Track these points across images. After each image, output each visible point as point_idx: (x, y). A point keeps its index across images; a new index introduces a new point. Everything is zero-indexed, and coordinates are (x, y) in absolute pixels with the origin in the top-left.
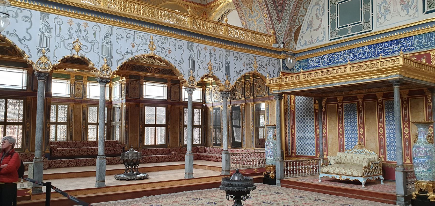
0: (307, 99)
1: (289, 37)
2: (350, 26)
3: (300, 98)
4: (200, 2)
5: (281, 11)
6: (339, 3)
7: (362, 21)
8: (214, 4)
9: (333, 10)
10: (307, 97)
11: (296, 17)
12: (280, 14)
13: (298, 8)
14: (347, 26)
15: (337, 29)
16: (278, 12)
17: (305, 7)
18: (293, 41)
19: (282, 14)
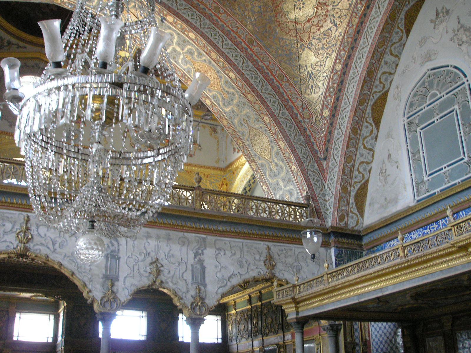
0: (390, 326)
1: (342, 203)
2: (447, 169)
3: (378, 325)
4: (215, 165)
5: (325, 159)
6: (422, 129)
7: (464, 156)
8: (236, 165)
9: (414, 142)
10: (389, 323)
11: (354, 164)
12: (324, 163)
13: (353, 149)
14: (442, 169)
15: (425, 178)
16: (318, 161)
17: (368, 146)
18: (356, 211)
19: (328, 164)
